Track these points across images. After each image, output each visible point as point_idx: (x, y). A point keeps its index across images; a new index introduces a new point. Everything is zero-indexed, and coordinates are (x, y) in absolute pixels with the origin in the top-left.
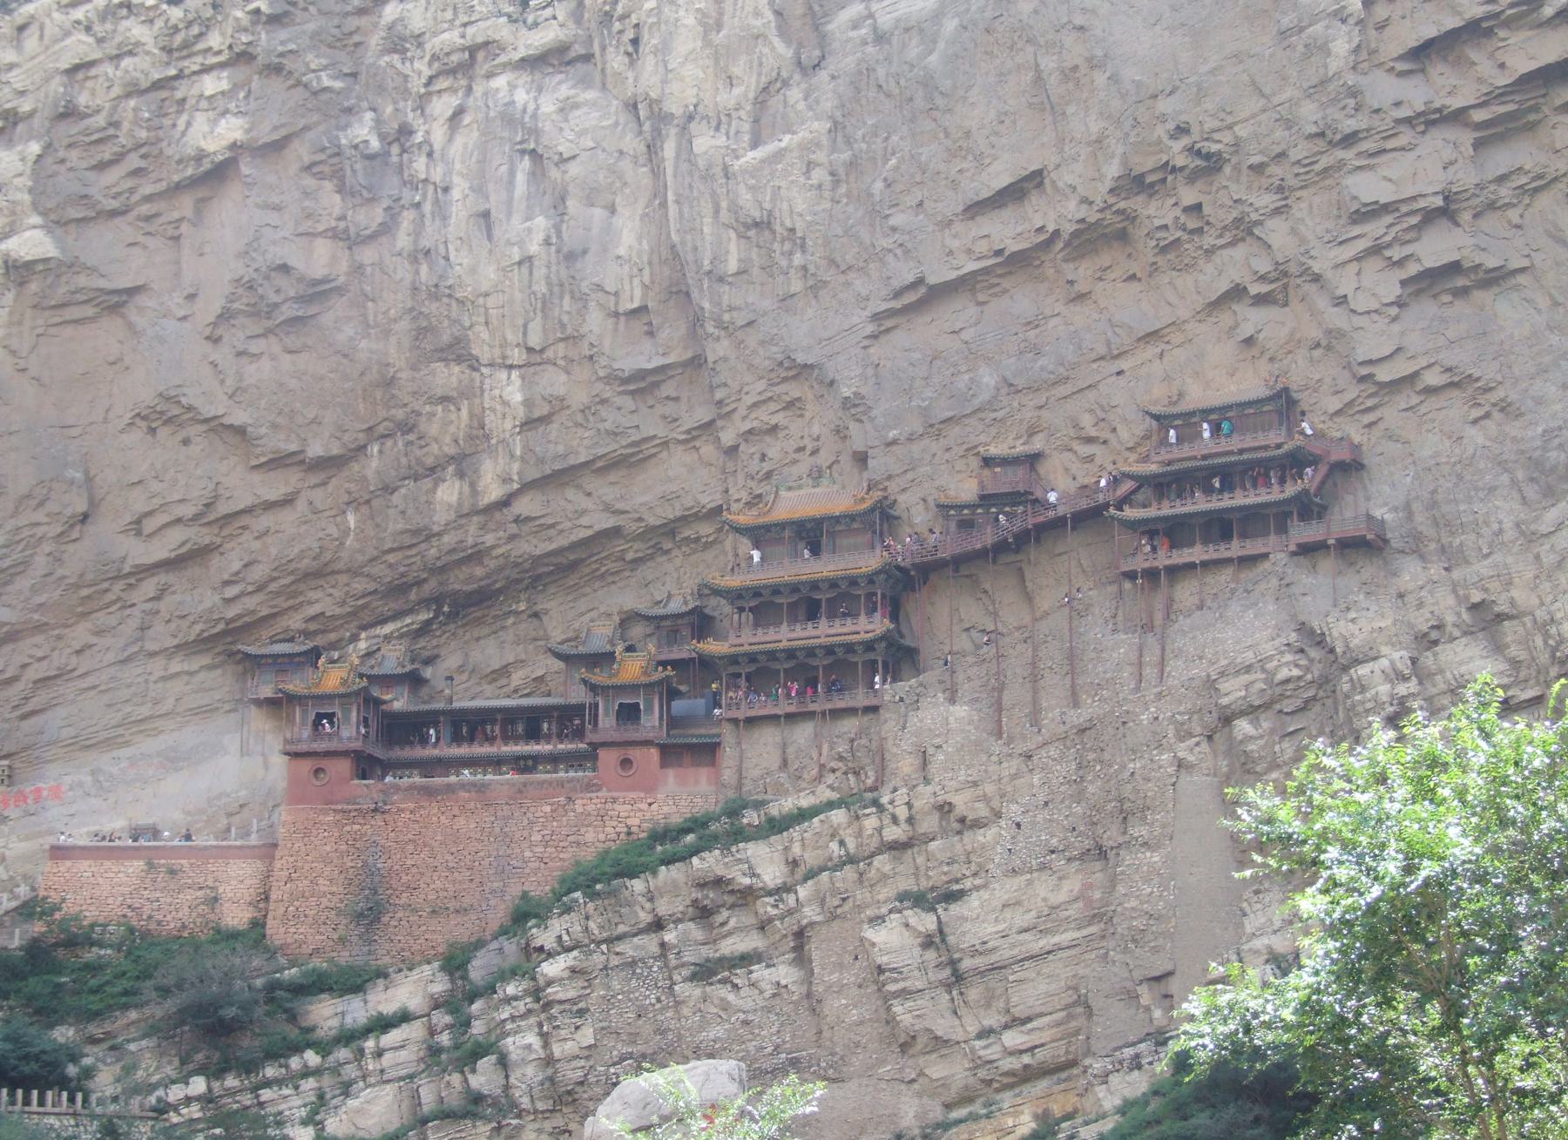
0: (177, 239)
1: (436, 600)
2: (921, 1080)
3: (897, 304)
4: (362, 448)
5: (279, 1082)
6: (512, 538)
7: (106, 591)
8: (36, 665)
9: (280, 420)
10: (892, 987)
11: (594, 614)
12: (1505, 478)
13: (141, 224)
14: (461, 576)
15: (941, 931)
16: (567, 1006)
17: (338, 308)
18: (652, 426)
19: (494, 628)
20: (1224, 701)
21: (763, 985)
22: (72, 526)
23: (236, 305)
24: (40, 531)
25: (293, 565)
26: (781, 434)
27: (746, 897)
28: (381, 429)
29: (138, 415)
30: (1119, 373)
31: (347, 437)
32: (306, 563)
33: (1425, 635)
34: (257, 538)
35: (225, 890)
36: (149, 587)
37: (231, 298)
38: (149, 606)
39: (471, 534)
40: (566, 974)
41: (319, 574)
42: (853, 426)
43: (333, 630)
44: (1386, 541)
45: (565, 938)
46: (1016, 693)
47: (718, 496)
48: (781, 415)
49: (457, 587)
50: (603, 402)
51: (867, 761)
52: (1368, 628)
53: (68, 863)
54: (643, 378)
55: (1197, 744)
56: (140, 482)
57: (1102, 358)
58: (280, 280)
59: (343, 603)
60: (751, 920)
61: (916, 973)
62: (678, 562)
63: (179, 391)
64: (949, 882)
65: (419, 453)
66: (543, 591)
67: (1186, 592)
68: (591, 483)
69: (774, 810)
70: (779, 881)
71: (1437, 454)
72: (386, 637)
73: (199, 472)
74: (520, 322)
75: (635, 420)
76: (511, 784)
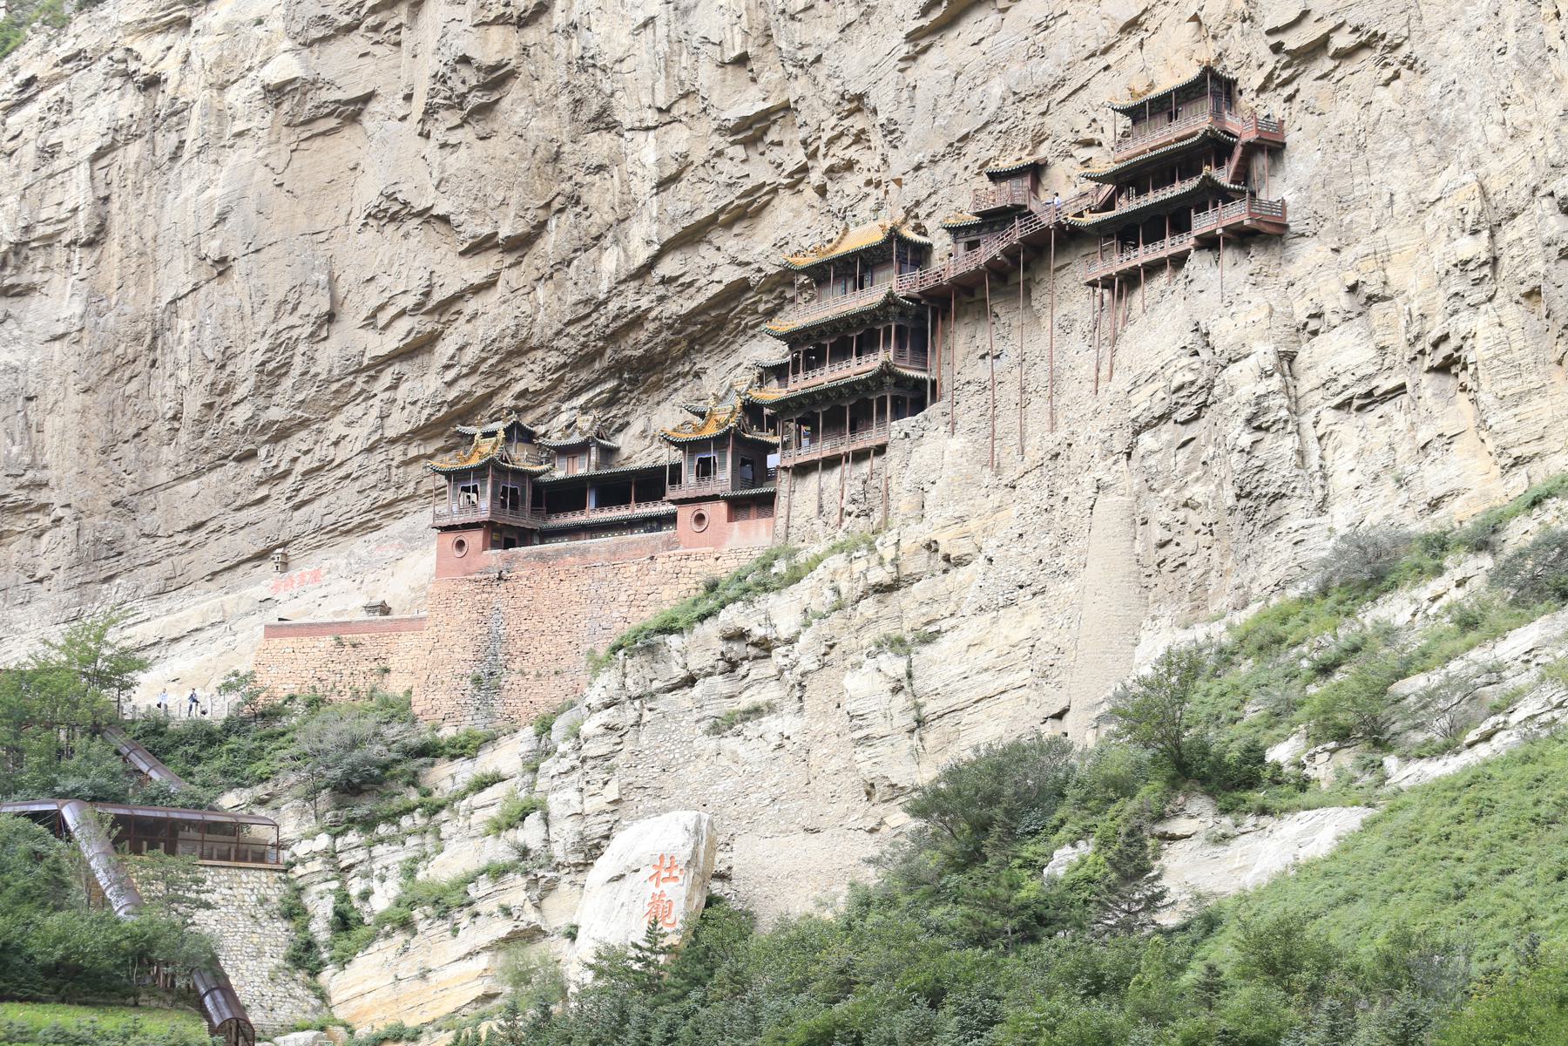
0: (398, 44)
1: (616, 369)
2: (884, 829)
3: (925, 22)
4: (541, 227)
5: (390, 840)
6: (661, 299)
7: (352, 384)
8: (303, 458)
9: (477, 206)
10: (859, 734)
11: (740, 370)
12: (1405, 143)
13: (370, 34)
14: (631, 342)
15: (910, 675)
16: (599, 761)
17: (515, 90)
18: (760, 171)
19: (670, 390)
20: (1133, 414)
21: (767, 736)
22: (321, 326)
23: (436, 100)
24: (295, 333)
25: (496, 345)
26: (856, 168)
27: (765, 647)
28: (556, 205)
29: (369, 215)
30: (1106, 68)
31: (529, 216)
32: (508, 343)
33: (1306, 325)
34: (468, 321)
35: (393, 663)
36: (387, 378)
37: (433, 93)
38: (387, 394)
39: (632, 299)
40: (602, 730)
41: (520, 352)
42: (891, 153)
43: (540, 405)
44: (1286, 227)
45: (604, 695)
46: (1008, 420)
47: (818, 238)
48: (854, 148)
49: (628, 353)
50: (720, 154)
51: (877, 502)
52: (1241, 324)
53: (277, 640)
54: (750, 127)
55: (1115, 462)
56: (372, 279)
57: (1093, 55)
58: (465, 71)
59: (542, 379)
60: (774, 672)
61: (881, 720)
62: (801, 308)
63: (396, 188)
64: (928, 623)
65: (585, 223)
66: (699, 351)
67: (1137, 299)
68: (717, 237)
69: (801, 559)
70: (793, 631)
71: (1343, 123)
72: (581, 408)
73: (417, 264)
74: (649, 84)
75: (746, 169)
76: (646, 542)
